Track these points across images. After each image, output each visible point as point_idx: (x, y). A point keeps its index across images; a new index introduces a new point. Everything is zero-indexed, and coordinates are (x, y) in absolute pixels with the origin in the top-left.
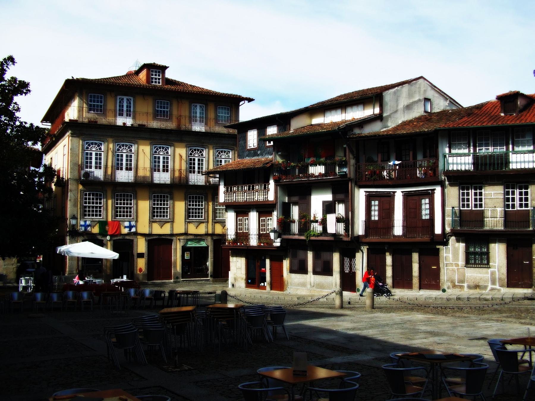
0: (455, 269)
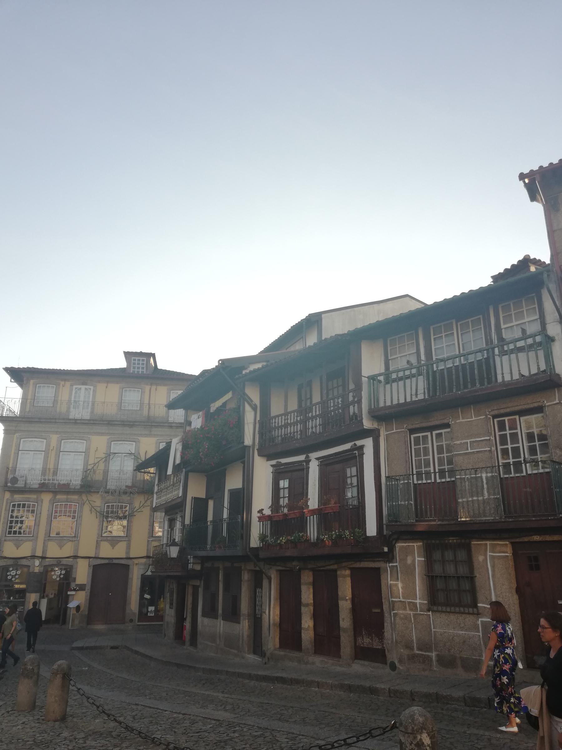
0: (410, 614)
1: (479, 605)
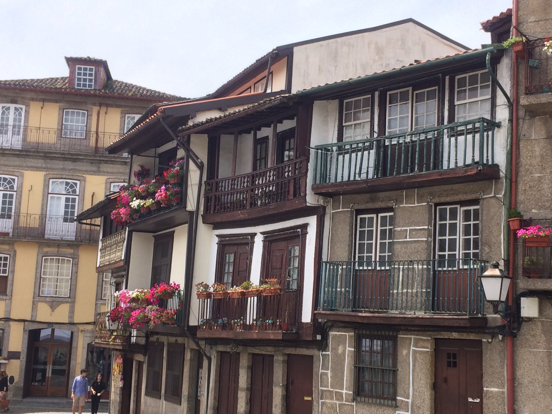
0: (336, 404)
1: (398, 398)
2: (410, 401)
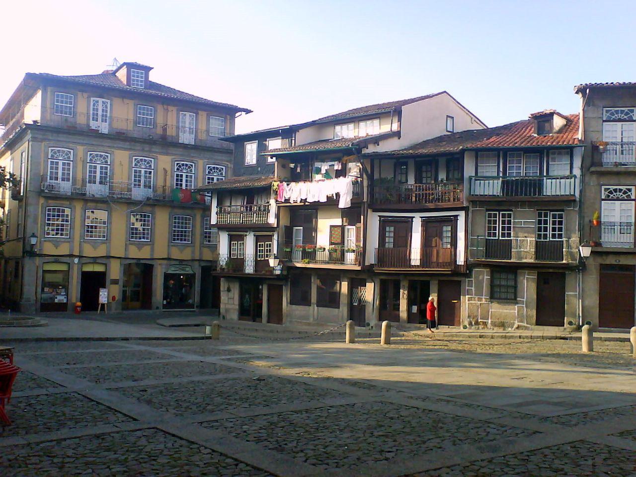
2: (525, 300)
